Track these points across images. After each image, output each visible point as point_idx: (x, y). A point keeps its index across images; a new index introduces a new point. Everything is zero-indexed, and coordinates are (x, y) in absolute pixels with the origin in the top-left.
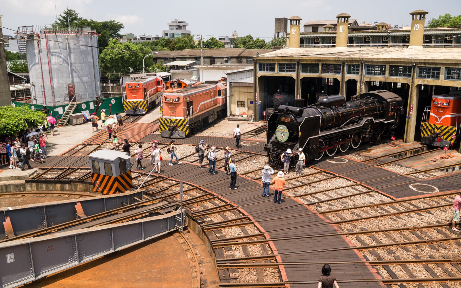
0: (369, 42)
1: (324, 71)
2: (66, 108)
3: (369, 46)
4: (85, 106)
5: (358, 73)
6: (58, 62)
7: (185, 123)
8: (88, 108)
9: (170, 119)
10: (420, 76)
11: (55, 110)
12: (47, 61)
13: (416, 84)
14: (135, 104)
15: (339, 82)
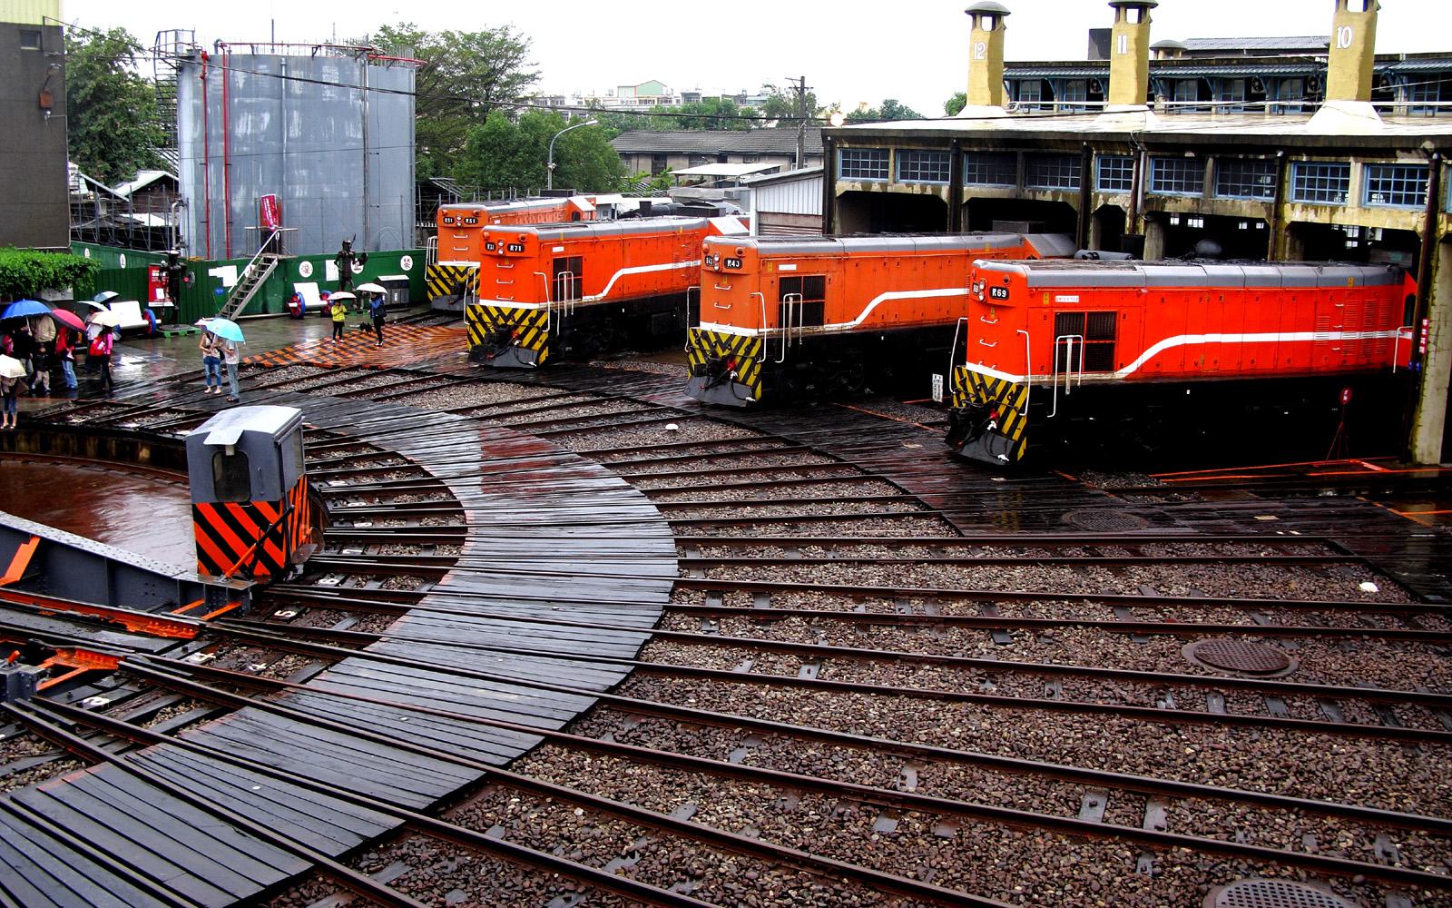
0: (1262, 98)
1: (1033, 179)
2: (247, 272)
3: (1262, 108)
4: (311, 272)
5: (1127, 186)
6: (251, 134)
7: (540, 323)
8: (318, 276)
9: (498, 309)
10: (1299, 195)
11: (212, 272)
12: (222, 132)
13: (1287, 221)
14: (462, 275)
15: (1074, 213)
